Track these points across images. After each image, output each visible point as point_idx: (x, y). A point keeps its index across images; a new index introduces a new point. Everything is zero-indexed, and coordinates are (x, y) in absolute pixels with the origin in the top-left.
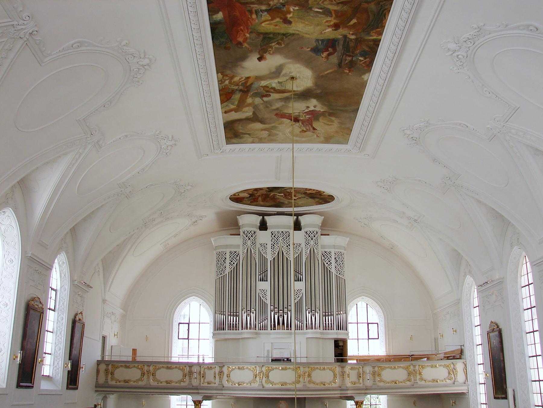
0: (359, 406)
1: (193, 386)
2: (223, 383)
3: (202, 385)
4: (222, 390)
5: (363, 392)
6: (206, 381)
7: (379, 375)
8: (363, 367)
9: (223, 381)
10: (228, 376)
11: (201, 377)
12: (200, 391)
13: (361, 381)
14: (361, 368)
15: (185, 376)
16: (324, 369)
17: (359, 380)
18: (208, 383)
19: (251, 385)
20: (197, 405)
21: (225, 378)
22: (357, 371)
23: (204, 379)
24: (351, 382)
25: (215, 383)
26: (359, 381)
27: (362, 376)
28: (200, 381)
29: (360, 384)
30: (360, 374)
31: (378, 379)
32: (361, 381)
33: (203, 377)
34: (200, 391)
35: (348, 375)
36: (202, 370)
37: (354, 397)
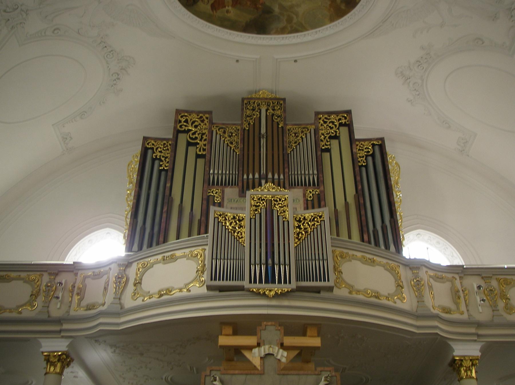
0: (466, 371)
1: (49, 316)
2: (122, 301)
3: (72, 313)
4: (118, 315)
5: (473, 330)
6: (84, 303)
7: (504, 296)
8: (461, 278)
9: (123, 297)
10: (138, 283)
11: (75, 293)
12: (65, 326)
13: (463, 308)
14: (458, 278)
15: (34, 296)
16: (372, 262)
17: (457, 304)
18: (89, 307)
19: (190, 291)
20: (52, 365)
21: (131, 288)
22: (448, 285)
23: (80, 300)
24: (439, 306)
25: (104, 304)
26: (458, 308)
27: (461, 294)
28: (70, 307)
29: (462, 313)
30: (458, 291)
31: (501, 304)
32: (463, 308)
33: (78, 294)
34: (65, 326)
35: (431, 287)
36: (79, 278)
37: (451, 343)
